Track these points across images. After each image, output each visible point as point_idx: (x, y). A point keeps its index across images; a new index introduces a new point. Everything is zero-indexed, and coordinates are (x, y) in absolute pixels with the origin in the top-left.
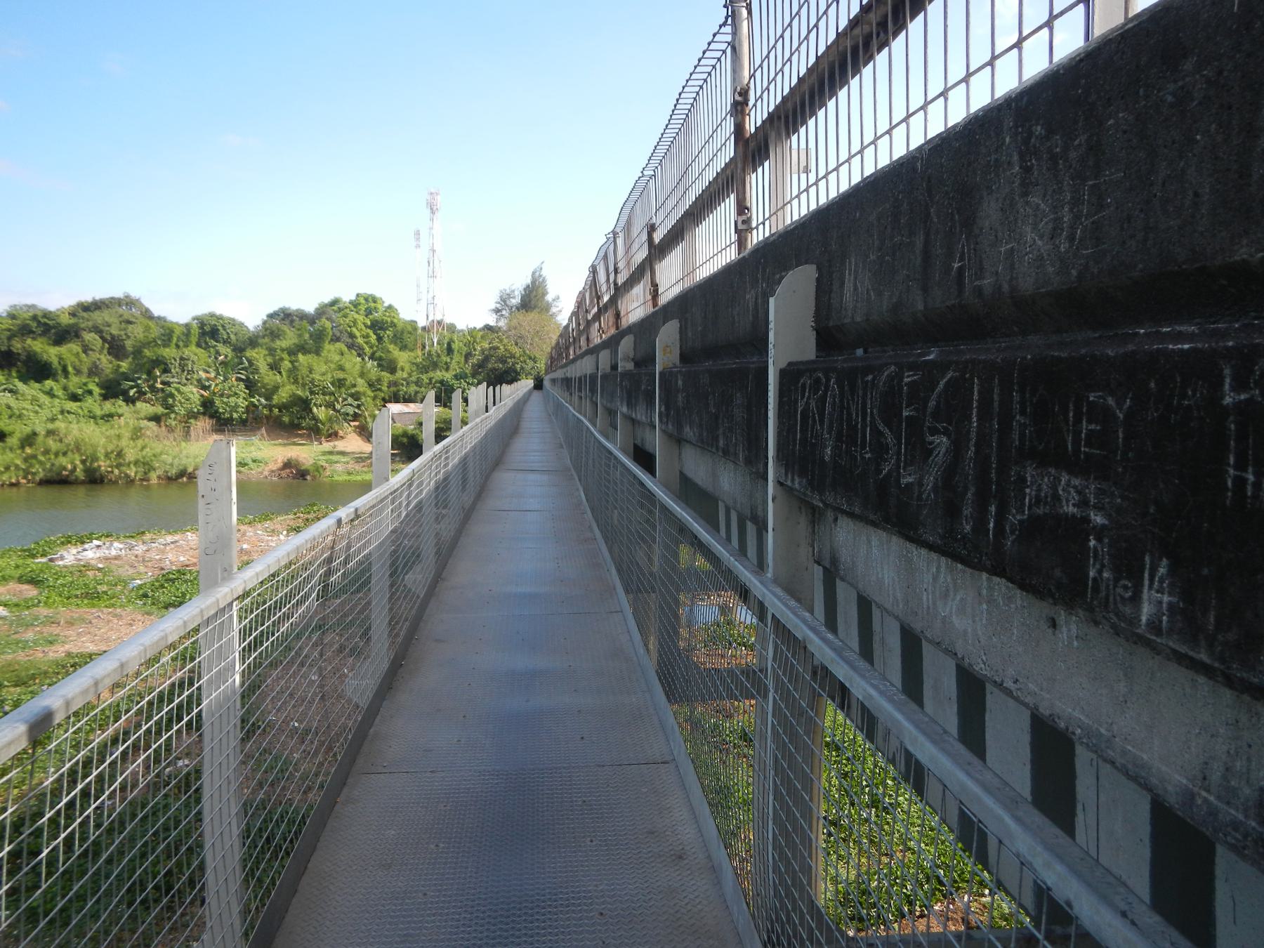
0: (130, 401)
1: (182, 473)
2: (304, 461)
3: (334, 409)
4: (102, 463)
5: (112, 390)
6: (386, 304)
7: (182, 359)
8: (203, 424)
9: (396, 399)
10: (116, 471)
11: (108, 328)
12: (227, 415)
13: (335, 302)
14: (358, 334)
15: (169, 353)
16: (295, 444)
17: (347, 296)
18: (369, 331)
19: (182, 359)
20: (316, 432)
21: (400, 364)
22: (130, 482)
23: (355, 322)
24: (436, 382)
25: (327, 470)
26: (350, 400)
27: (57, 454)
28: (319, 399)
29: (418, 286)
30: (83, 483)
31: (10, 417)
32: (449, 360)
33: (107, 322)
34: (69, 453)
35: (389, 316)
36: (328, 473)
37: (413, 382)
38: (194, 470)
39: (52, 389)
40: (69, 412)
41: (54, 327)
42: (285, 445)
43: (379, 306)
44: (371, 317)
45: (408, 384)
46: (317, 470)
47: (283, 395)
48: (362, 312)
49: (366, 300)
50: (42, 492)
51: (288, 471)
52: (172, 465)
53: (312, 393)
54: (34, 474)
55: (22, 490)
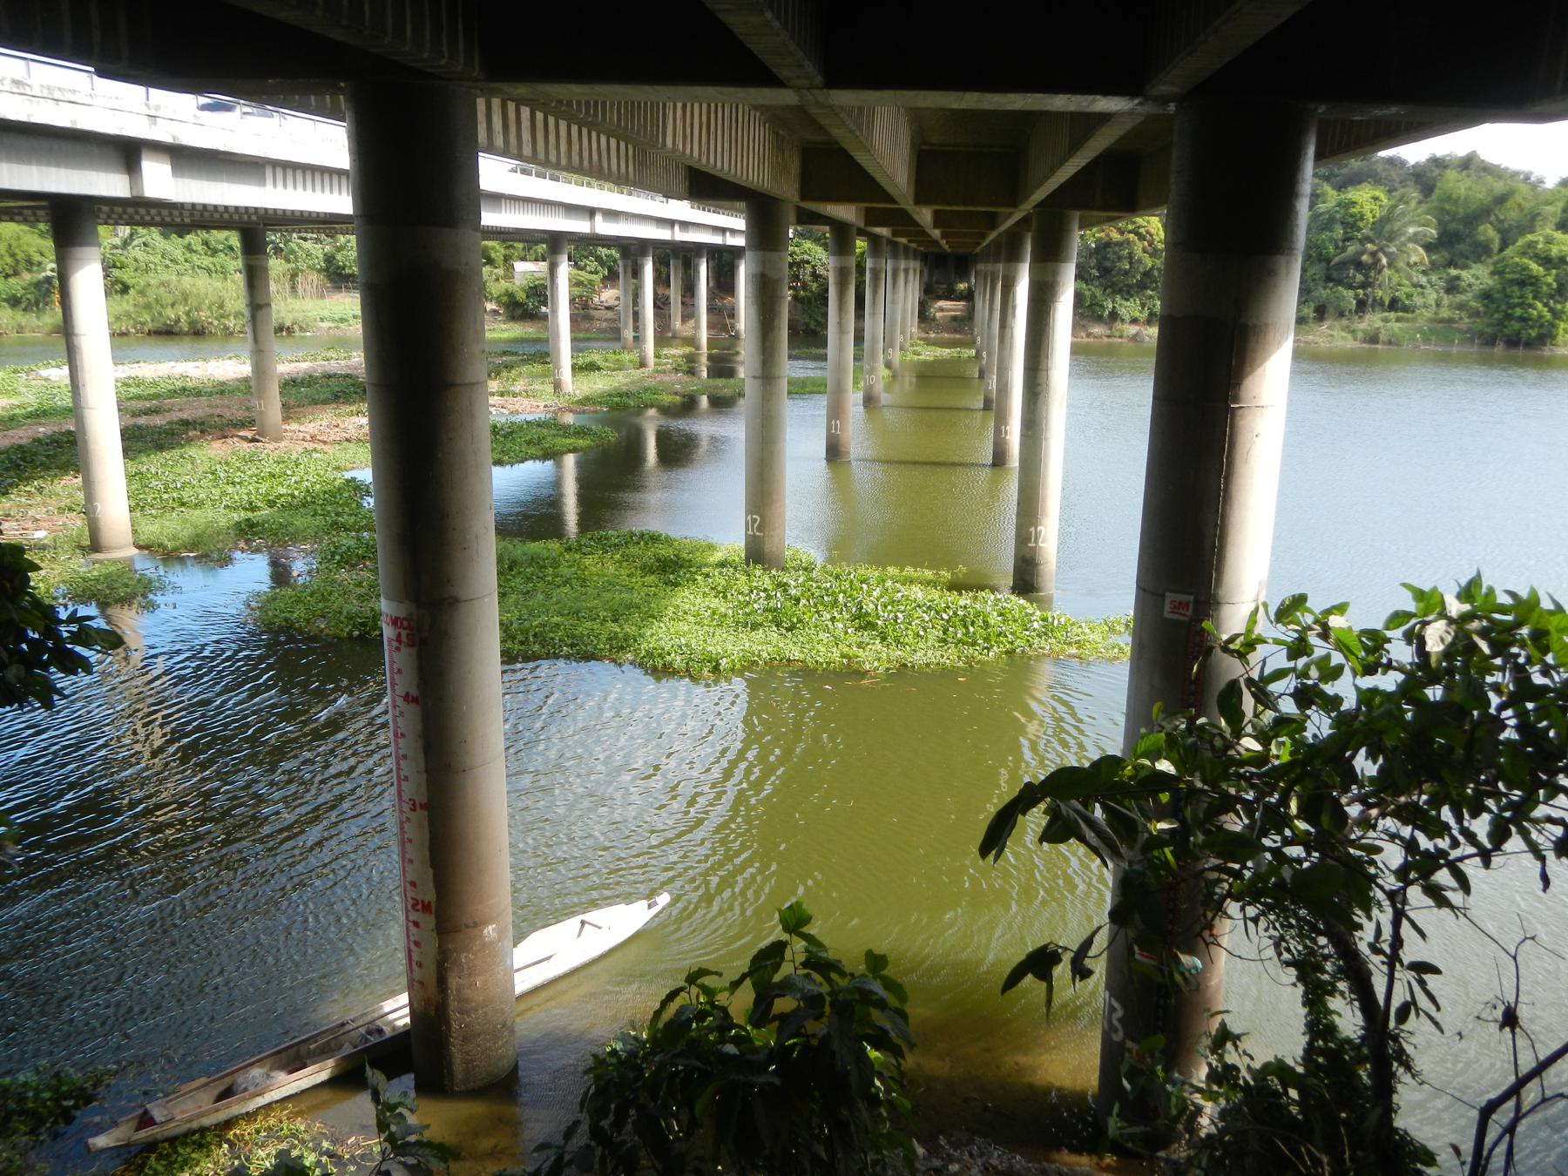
8: (314, 277)
10: (216, 323)
30: (187, 334)
31: (136, 270)
39: (190, 244)
40: (199, 267)
50: (153, 339)
54: (143, 324)
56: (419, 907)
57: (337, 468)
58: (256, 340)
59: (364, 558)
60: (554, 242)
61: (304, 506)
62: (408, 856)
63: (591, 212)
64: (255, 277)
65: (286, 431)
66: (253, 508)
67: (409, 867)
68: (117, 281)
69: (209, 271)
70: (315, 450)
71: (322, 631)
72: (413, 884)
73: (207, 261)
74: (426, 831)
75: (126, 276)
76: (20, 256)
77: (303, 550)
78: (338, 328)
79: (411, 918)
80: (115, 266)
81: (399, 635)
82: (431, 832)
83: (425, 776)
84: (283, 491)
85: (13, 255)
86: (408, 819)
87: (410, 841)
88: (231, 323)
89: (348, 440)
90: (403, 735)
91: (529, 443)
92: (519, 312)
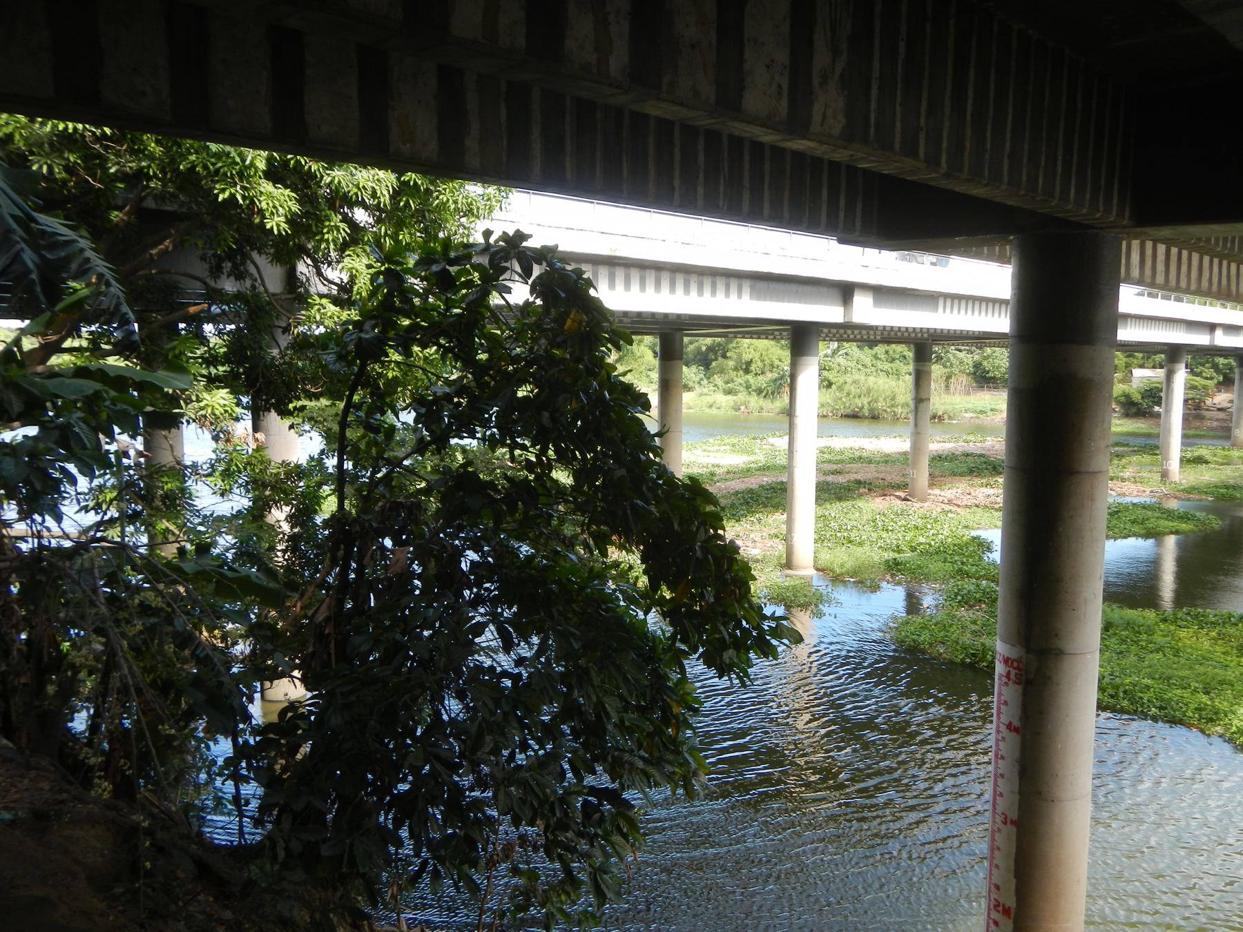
8: (964, 379)
12: (991, 375)
30: (866, 418)
40: (882, 371)
56: (1000, 909)
57: (966, 527)
58: (916, 425)
59: (980, 601)
60: (1173, 353)
61: (937, 553)
62: (995, 862)
63: (1212, 327)
64: (920, 378)
65: (930, 494)
66: (899, 551)
67: (995, 871)
68: (825, 379)
69: (888, 373)
70: (950, 511)
71: (941, 654)
72: (997, 887)
73: (887, 366)
74: (1014, 845)
75: (830, 376)
76: (768, 361)
77: (933, 589)
78: (978, 418)
79: (992, 916)
80: (825, 369)
81: (1008, 674)
82: (1017, 847)
83: (1017, 797)
84: (922, 540)
85: (763, 361)
86: (999, 830)
87: (999, 849)
88: (899, 410)
89: (977, 506)
90: (1003, 758)
91: (1133, 522)
92: (1134, 410)
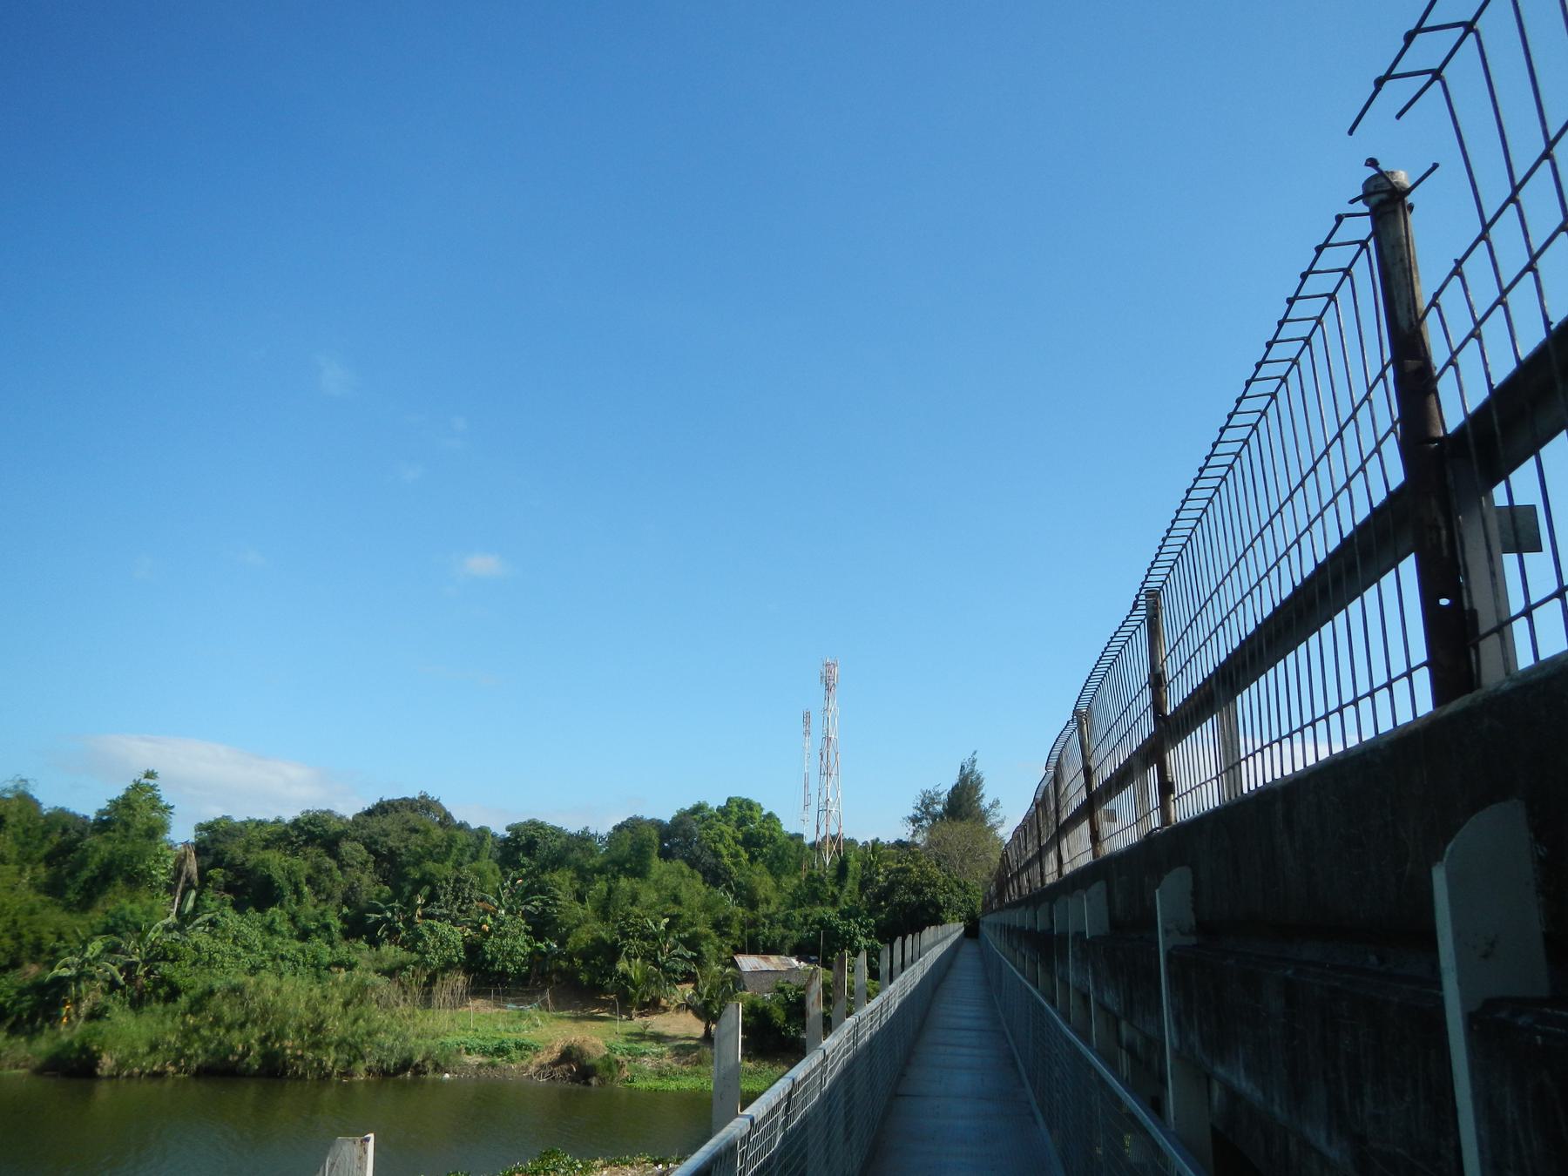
0: (374, 943)
1: (406, 1065)
2: (592, 1051)
3: (656, 964)
4: (288, 1043)
5: (358, 927)
6: (765, 813)
7: (457, 880)
9: (752, 948)
11: (383, 839)
12: (497, 967)
13: (698, 809)
14: (725, 852)
15: (446, 870)
16: (593, 1018)
17: (716, 801)
18: (739, 847)
19: (457, 880)
20: (629, 999)
21: (761, 893)
22: (324, 1077)
23: (721, 835)
24: (814, 922)
25: (625, 1069)
26: (680, 950)
27: (229, 1028)
28: (635, 944)
29: (806, 786)
30: (257, 1075)
32: (836, 892)
33: (384, 830)
34: (249, 1025)
35: (768, 829)
36: (627, 1074)
37: (779, 921)
38: (423, 1061)
40: (283, 958)
41: (321, 836)
42: (577, 1019)
43: (756, 815)
44: (744, 829)
45: (771, 924)
46: (609, 1068)
47: (582, 937)
48: (732, 823)
49: (740, 806)
51: (565, 1067)
52: (391, 1050)
53: (625, 935)
54: (190, 1058)
55: (169, 1084)
68: (164, 981)
69: (295, 961)
88: (330, 1059)
